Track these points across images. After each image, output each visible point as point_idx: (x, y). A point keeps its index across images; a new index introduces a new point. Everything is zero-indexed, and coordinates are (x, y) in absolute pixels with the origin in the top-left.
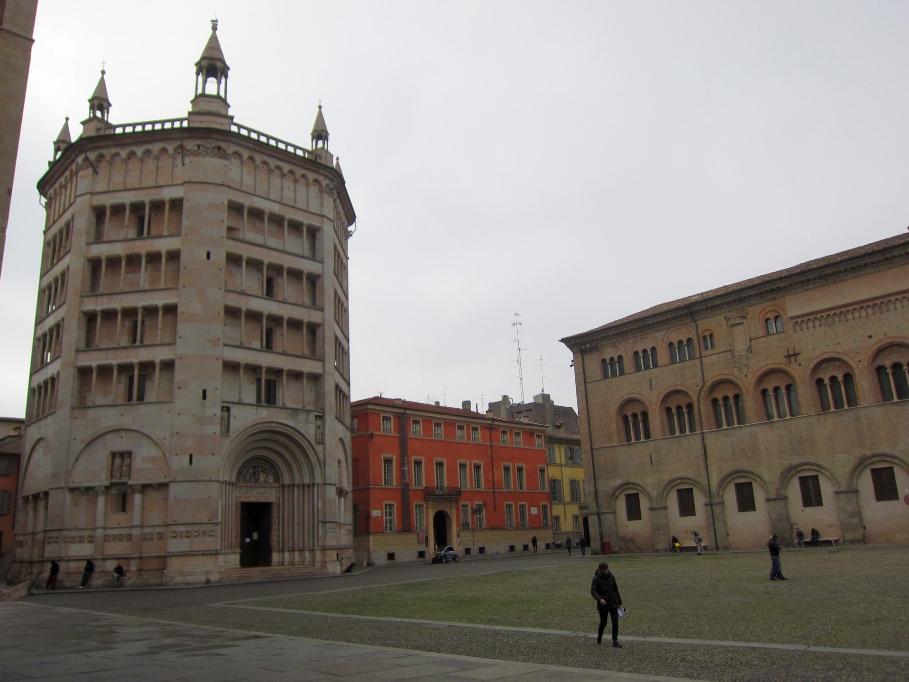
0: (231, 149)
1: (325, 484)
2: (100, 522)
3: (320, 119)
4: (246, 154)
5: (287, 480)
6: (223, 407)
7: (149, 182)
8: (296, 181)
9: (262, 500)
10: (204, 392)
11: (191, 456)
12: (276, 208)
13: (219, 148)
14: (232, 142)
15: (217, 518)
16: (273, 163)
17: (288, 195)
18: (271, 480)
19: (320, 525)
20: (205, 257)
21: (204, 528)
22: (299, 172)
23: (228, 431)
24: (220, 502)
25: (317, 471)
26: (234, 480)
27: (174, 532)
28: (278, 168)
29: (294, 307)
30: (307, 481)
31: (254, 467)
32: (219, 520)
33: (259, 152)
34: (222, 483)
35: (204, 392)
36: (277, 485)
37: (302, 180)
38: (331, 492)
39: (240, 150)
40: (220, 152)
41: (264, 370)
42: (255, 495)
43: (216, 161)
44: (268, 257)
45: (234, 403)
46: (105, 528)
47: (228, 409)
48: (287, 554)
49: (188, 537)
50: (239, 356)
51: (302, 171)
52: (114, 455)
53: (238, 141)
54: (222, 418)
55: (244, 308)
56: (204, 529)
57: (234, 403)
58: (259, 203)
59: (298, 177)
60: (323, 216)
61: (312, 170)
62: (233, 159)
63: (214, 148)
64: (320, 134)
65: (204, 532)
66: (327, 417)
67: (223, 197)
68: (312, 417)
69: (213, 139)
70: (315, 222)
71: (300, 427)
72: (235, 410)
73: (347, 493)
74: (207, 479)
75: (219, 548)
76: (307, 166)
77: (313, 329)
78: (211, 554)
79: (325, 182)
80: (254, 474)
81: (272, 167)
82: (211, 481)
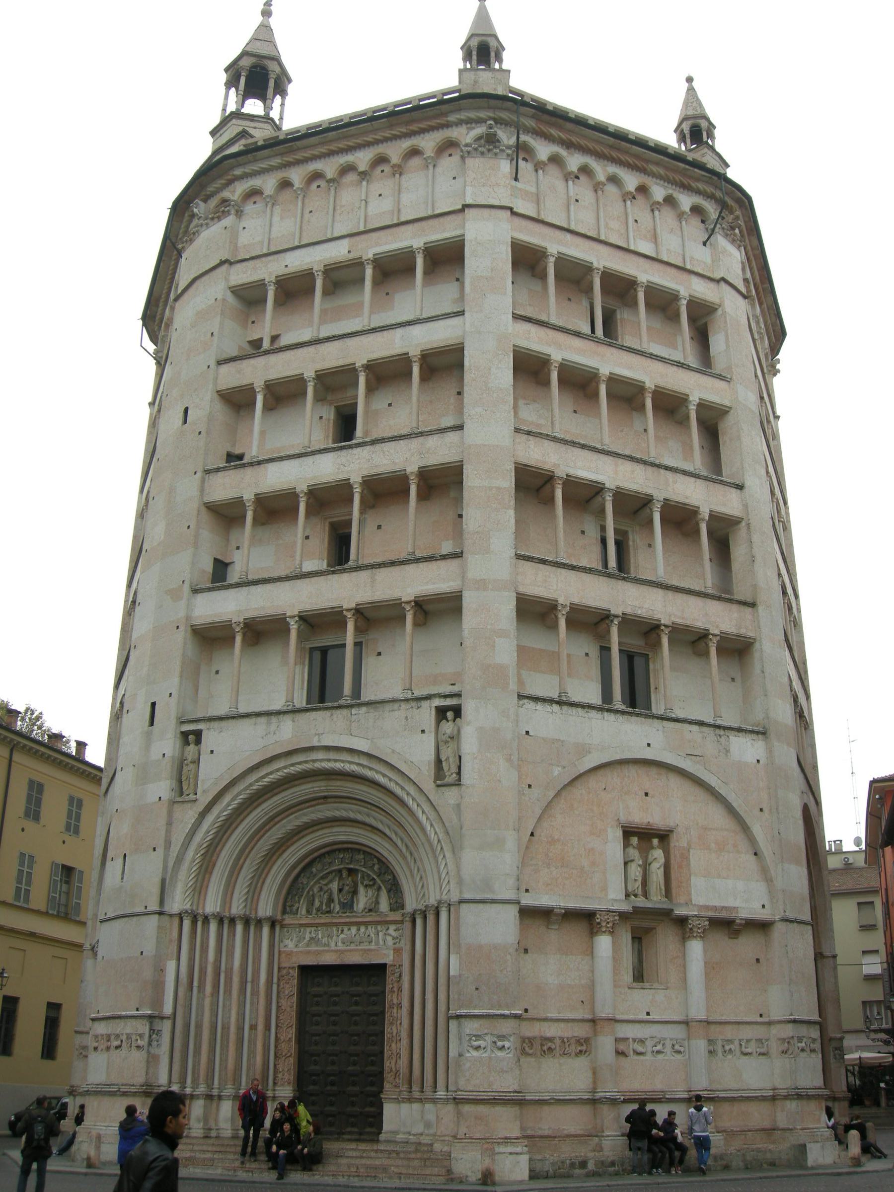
0: (239, 190)
4: (268, 184)
5: (411, 904)
6: (185, 735)
9: (355, 959)
10: (153, 705)
12: (339, 252)
15: (158, 1001)
18: (384, 906)
19: (453, 1024)
20: (181, 422)
24: (171, 966)
26: (266, 908)
29: (378, 447)
31: (340, 871)
32: (168, 1009)
33: (298, 162)
34: (180, 917)
35: (153, 705)
36: (396, 916)
37: (415, 162)
38: (497, 927)
39: (256, 182)
40: (223, 209)
42: (338, 946)
44: (306, 364)
45: (212, 719)
47: (198, 734)
50: (227, 607)
54: (181, 764)
55: (248, 496)
56: (128, 1030)
57: (212, 719)
58: (295, 262)
62: (249, 208)
64: (483, 50)
65: (129, 1037)
66: (469, 707)
68: (426, 714)
71: (383, 747)
72: (212, 737)
73: (762, 926)
74: (143, 910)
76: (414, 127)
79: (466, 135)
80: (340, 890)
81: (330, 173)
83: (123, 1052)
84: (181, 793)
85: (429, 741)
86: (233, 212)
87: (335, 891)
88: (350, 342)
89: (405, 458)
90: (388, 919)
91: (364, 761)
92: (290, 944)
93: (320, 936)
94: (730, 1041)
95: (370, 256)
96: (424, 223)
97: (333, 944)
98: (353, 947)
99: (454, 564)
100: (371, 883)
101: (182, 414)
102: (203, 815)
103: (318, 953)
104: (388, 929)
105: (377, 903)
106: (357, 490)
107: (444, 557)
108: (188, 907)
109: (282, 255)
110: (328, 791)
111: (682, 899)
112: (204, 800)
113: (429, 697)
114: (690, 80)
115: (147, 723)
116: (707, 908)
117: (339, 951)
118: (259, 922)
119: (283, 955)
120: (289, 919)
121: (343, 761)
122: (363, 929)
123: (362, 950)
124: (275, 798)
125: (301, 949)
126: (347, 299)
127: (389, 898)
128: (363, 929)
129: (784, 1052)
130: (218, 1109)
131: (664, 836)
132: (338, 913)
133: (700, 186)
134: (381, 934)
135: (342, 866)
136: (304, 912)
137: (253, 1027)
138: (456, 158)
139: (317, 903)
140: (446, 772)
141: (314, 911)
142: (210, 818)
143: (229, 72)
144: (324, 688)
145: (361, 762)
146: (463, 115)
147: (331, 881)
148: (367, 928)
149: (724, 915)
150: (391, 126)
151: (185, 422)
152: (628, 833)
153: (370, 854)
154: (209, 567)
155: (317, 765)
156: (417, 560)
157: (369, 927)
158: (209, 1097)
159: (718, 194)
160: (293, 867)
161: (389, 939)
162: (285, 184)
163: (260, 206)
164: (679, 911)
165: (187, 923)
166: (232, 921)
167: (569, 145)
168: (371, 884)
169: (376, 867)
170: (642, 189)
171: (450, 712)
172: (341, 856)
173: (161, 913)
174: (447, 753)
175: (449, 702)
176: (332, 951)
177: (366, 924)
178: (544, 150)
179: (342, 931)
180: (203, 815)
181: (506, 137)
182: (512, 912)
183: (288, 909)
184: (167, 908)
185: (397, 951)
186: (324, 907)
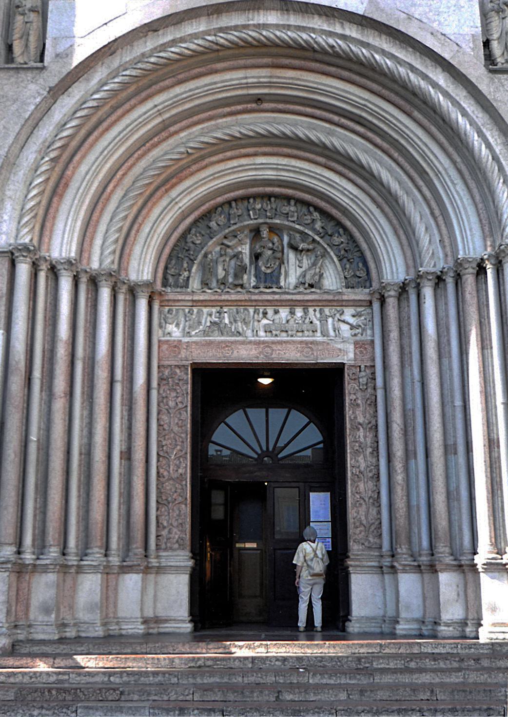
18: (332, 280)
36: (361, 294)
48: (409, 584)
80: (256, 257)
87: (247, 260)
90: (345, 298)
91: (352, 31)
93: (227, 321)
97: (249, 333)
98: (284, 337)
100: (311, 247)
103: (228, 344)
104: (342, 313)
105: (321, 276)
110: (270, 85)
117: (264, 342)
118: (133, 292)
119: (165, 347)
120: (171, 294)
121: (313, 30)
123: (301, 342)
124: (178, 90)
125: (194, 339)
127: (344, 269)
128: (299, 312)
130: (74, 588)
132: (255, 287)
134: (330, 320)
135: (261, 221)
136: (195, 284)
139: (221, 273)
141: (214, 284)
145: (347, 32)
147: (241, 242)
148: (306, 313)
157: (311, 310)
160: (184, 216)
161: (345, 327)
169: (318, 225)
172: (259, 206)
176: (250, 342)
177: (305, 305)
179: (265, 314)
183: (171, 280)
186: (231, 280)
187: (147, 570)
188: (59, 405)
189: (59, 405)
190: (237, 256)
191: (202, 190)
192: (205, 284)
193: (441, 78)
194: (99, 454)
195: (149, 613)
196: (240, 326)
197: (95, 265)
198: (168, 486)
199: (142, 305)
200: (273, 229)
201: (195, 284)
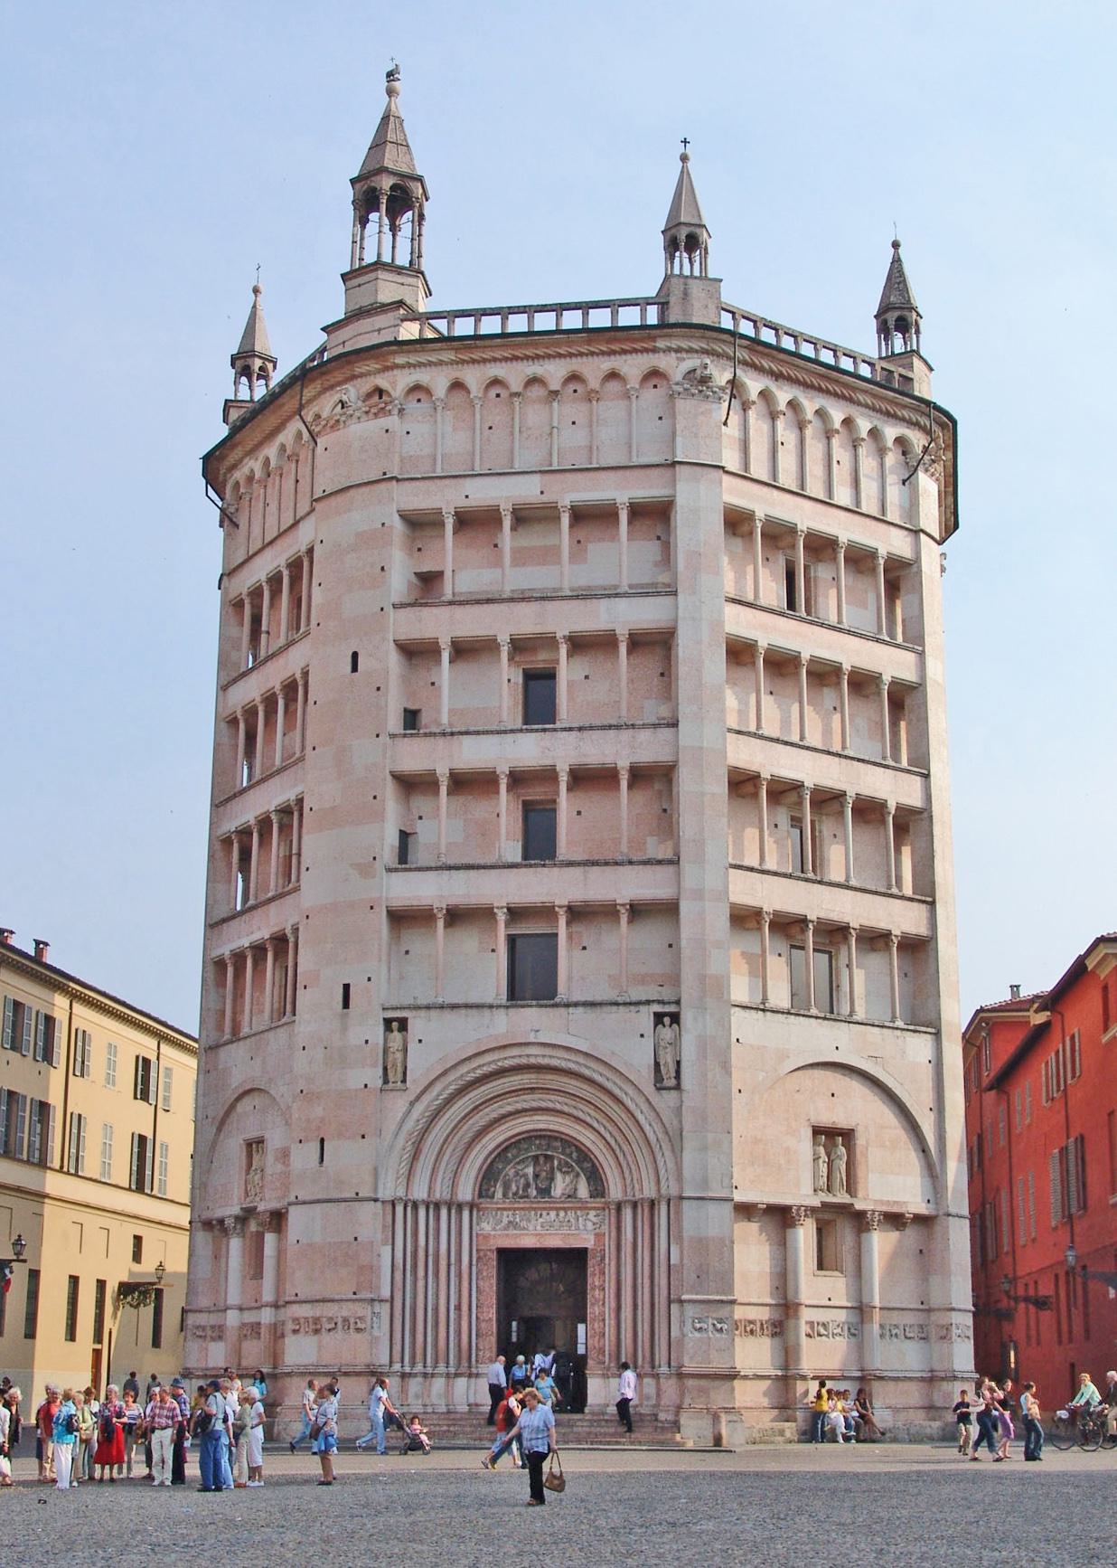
1: (682, 1198)
2: (234, 1297)
3: (684, 191)
4: (439, 381)
5: (615, 1191)
6: (388, 1023)
7: (288, 520)
8: (591, 397)
10: (347, 987)
11: (322, 1141)
12: (528, 490)
13: (380, 392)
14: (403, 367)
16: (515, 374)
17: (571, 442)
18: (583, 1191)
20: (349, 668)
21: (345, 1310)
22: (594, 368)
23: (404, 1081)
25: (666, 1160)
26: (466, 1192)
27: (296, 1320)
28: (534, 381)
29: (586, 734)
30: (649, 1191)
31: (536, 1158)
32: (386, 1293)
33: (474, 361)
35: (347, 987)
36: (599, 1202)
37: (613, 386)
39: (422, 376)
41: (501, 917)
42: (539, 1230)
43: (374, 426)
44: (503, 624)
46: (241, 1309)
47: (403, 1025)
49: (317, 1331)
51: (607, 364)
52: (249, 1145)
53: (413, 359)
56: (345, 1313)
58: (481, 493)
59: (594, 383)
60: (674, 464)
61: (636, 351)
62: (412, 406)
63: (369, 395)
64: (684, 238)
65: (345, 1320)
66: (687, 1016)
67: (386, 508)
68: (645, 1017)
69: (361, 375)
70: (647, 489)
72: (417, 1024)
75: (385, 1360)
76: (615, 347)
77: (655, 778)
78: (358, 1374)
80: (536, 1176)
81: (516, 384)
82: (357, 1199)
83: (339, 1334)
84: (386, 1081)
85: (648, 1044)
86: (395, 411)
88: (549, 605)
89: (618, 751)
91: (581, 1060)
92: (486, 1227)
94: (896, 1326)
95: (568, 504)
96: (628, 473)
99: (671, 869)
101: (349, 659)
102: (412, 1104)
106: (564, 779)
107: (660, 862)
108: (401, 1193)
109: (461, 481)
111: (860, 1195)
112: (414, 1086)
113: (648, 1002)
114: (896, 245)
115: (341, 1004)
116: (882, 1202)
118: (460, 1207)
120: (485, 1203)
122: (562, 1214)
126: (533, 538)
129: (943, 1338)
131: (848, 1135)
133: (906, 414)
136: (499, 1194)
137: (458, 1307)
138: (661, 391)
139: (514, 1188)
140: (667, 1077)
142: (420, 1108)
143: (358, 186)
144: (531, 980)
146: (674, 343)
149: (895, 1209)
150: (589, 342)
151: (355, 669)
152: (817, 1131)
153: (568, 1143)
154: (392, 839)
155: (533, 1061)
156: (631, 863)
158: (425, 1375)
159: (923, 421)
161: (590, 1226)
162: (457, 385)
163: (425, 405)
164: (859, 1206)
165: (399, 1209)
166: (437, 1206)
167: (777, 376)
168: (566, 1168)
170: (848, 422)
171: (669, 1018)
173: (376, 1200)
174: (667, 1059)
175: (668, 1009)
177: (565, 1209)
178: (754, 384)
180: (412, 1104)
181: (721, 376)
182: (728, 1207)
184: (380, 1195)
185: (599, 1236)
187: (470, 1376)
188: (421, 1284)
189: (421, 1284)
190: (525, 1175)
191: (502, 1138)
192: (505, 1195)
193: (631, 1091)
194: (442, 1309)
195: (472, 1401)
196: (524, 1224)
197: (438, 1196)
198: (483, 1325)
199: (466, 1214)
200: (546, 1156)
201: (499, 1194)
